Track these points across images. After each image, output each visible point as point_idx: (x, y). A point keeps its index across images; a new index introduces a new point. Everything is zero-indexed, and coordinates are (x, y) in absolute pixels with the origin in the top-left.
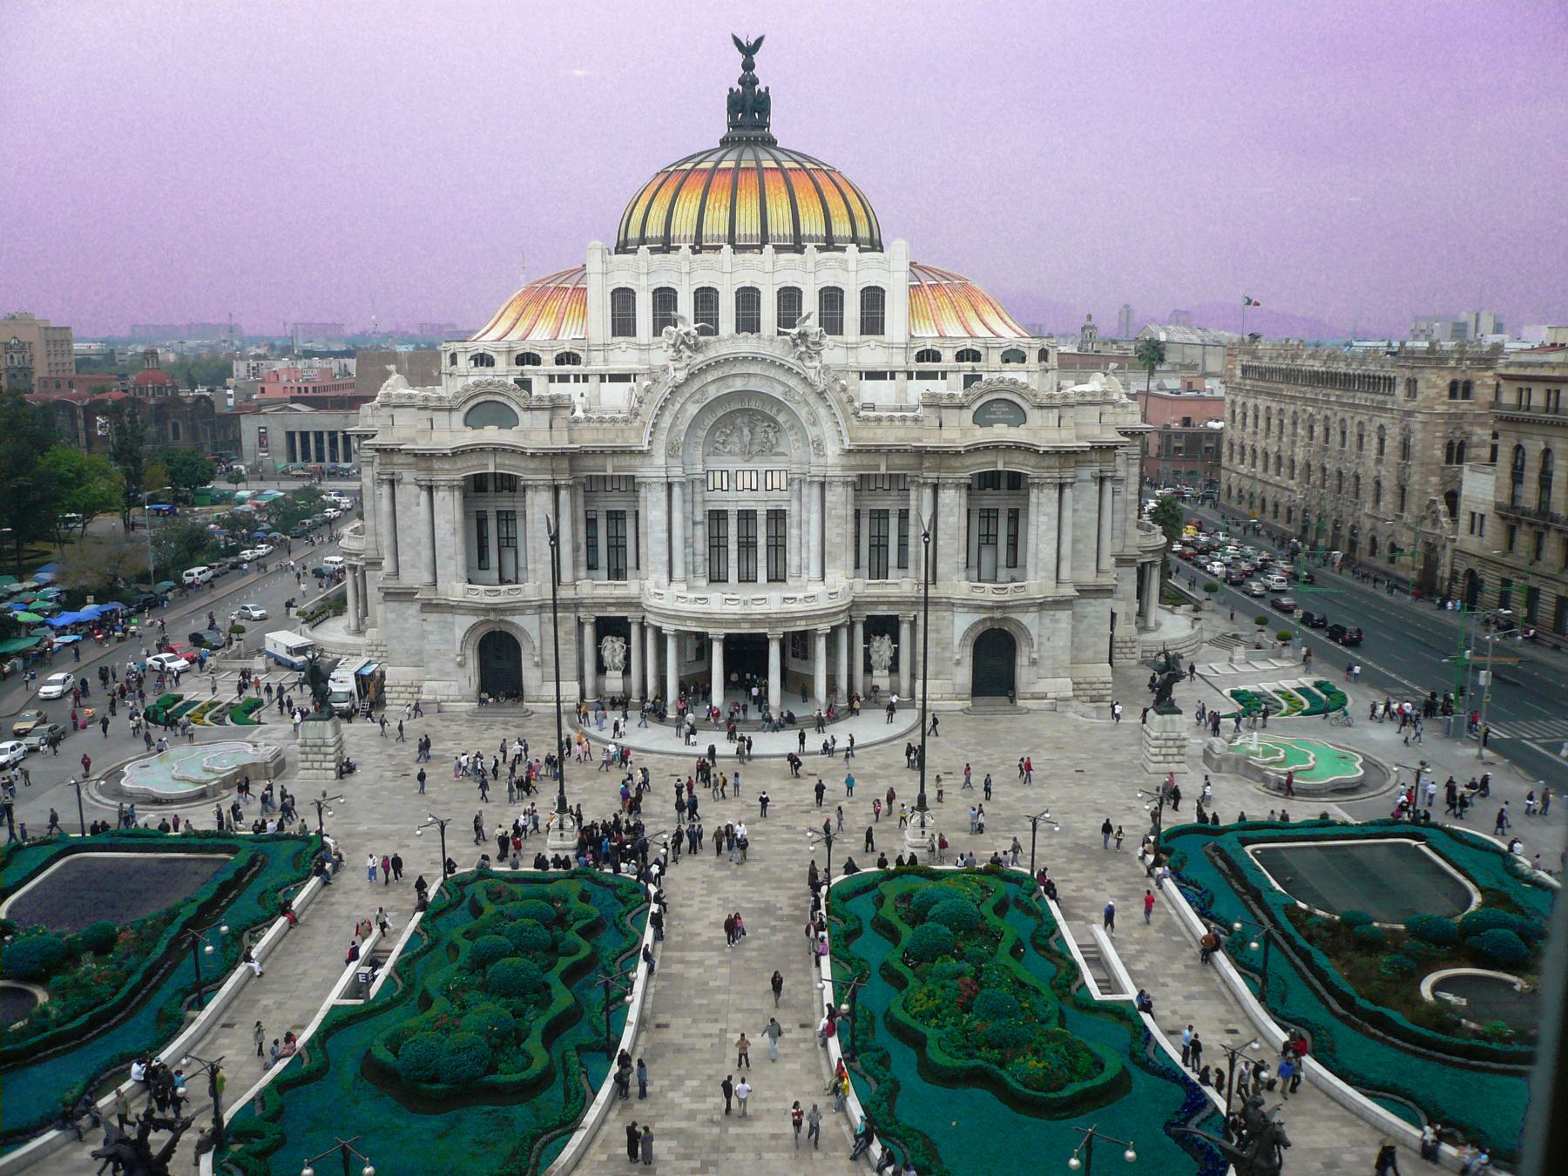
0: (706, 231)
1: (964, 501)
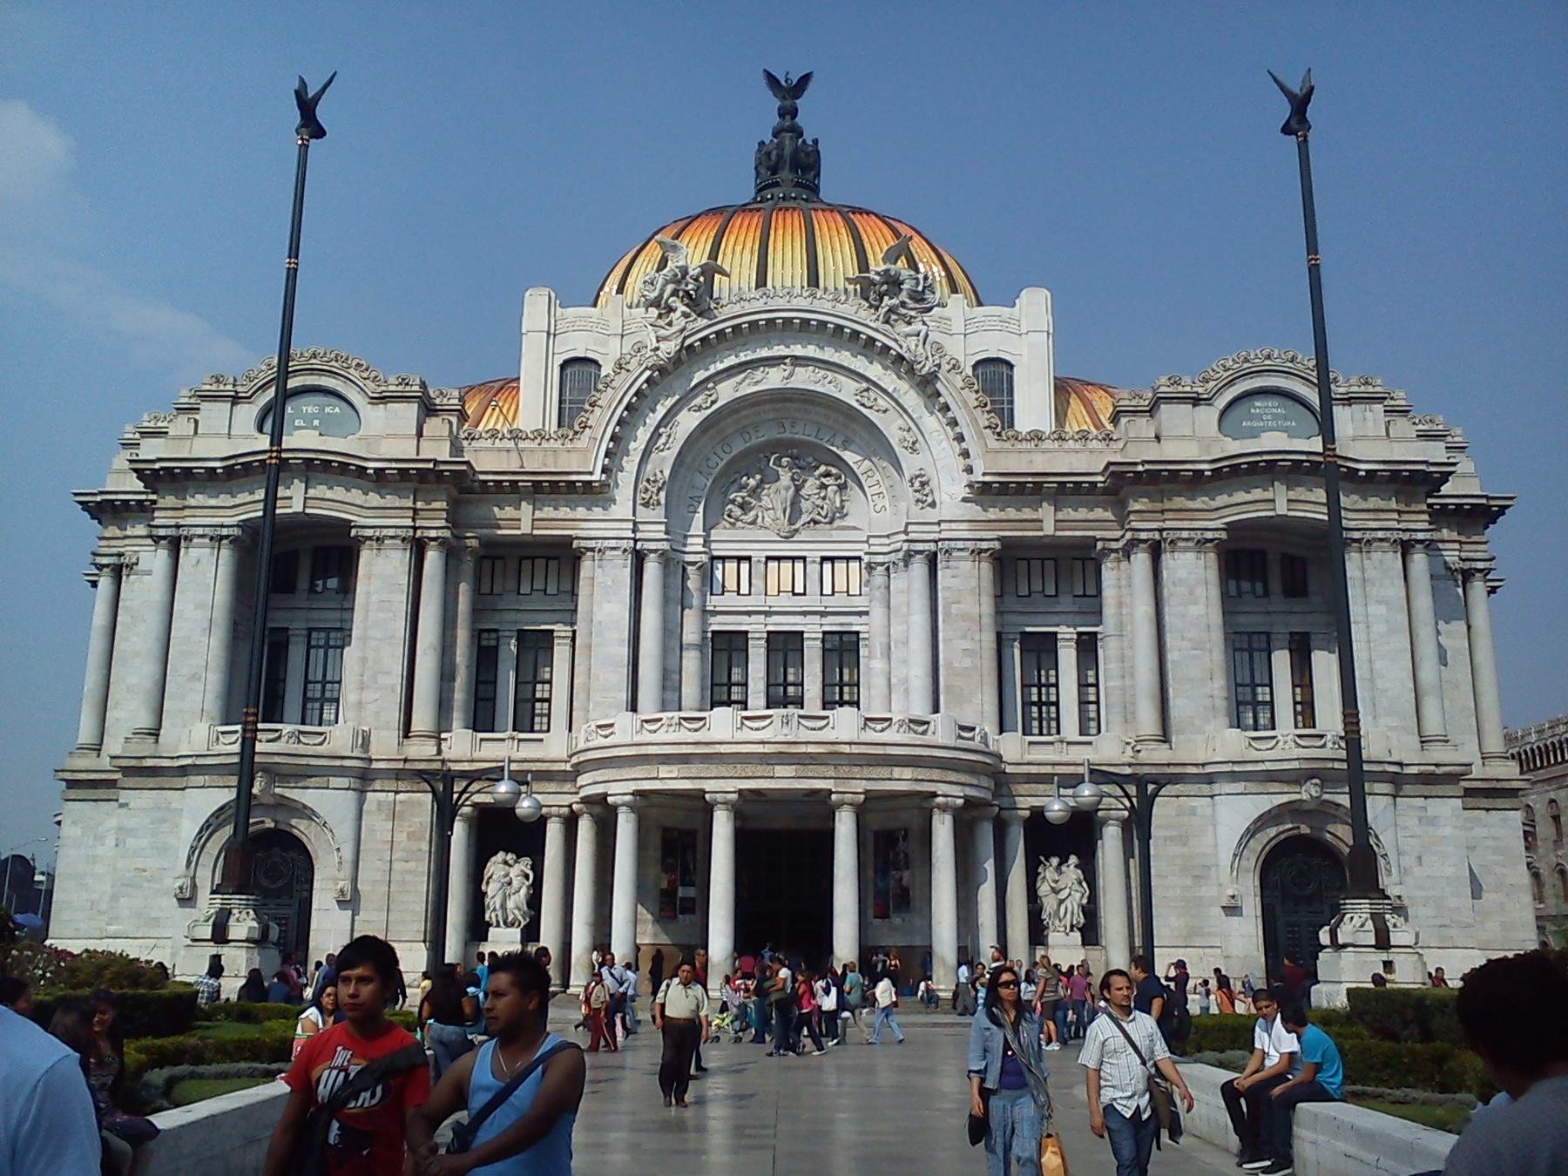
1: (1213, 575)
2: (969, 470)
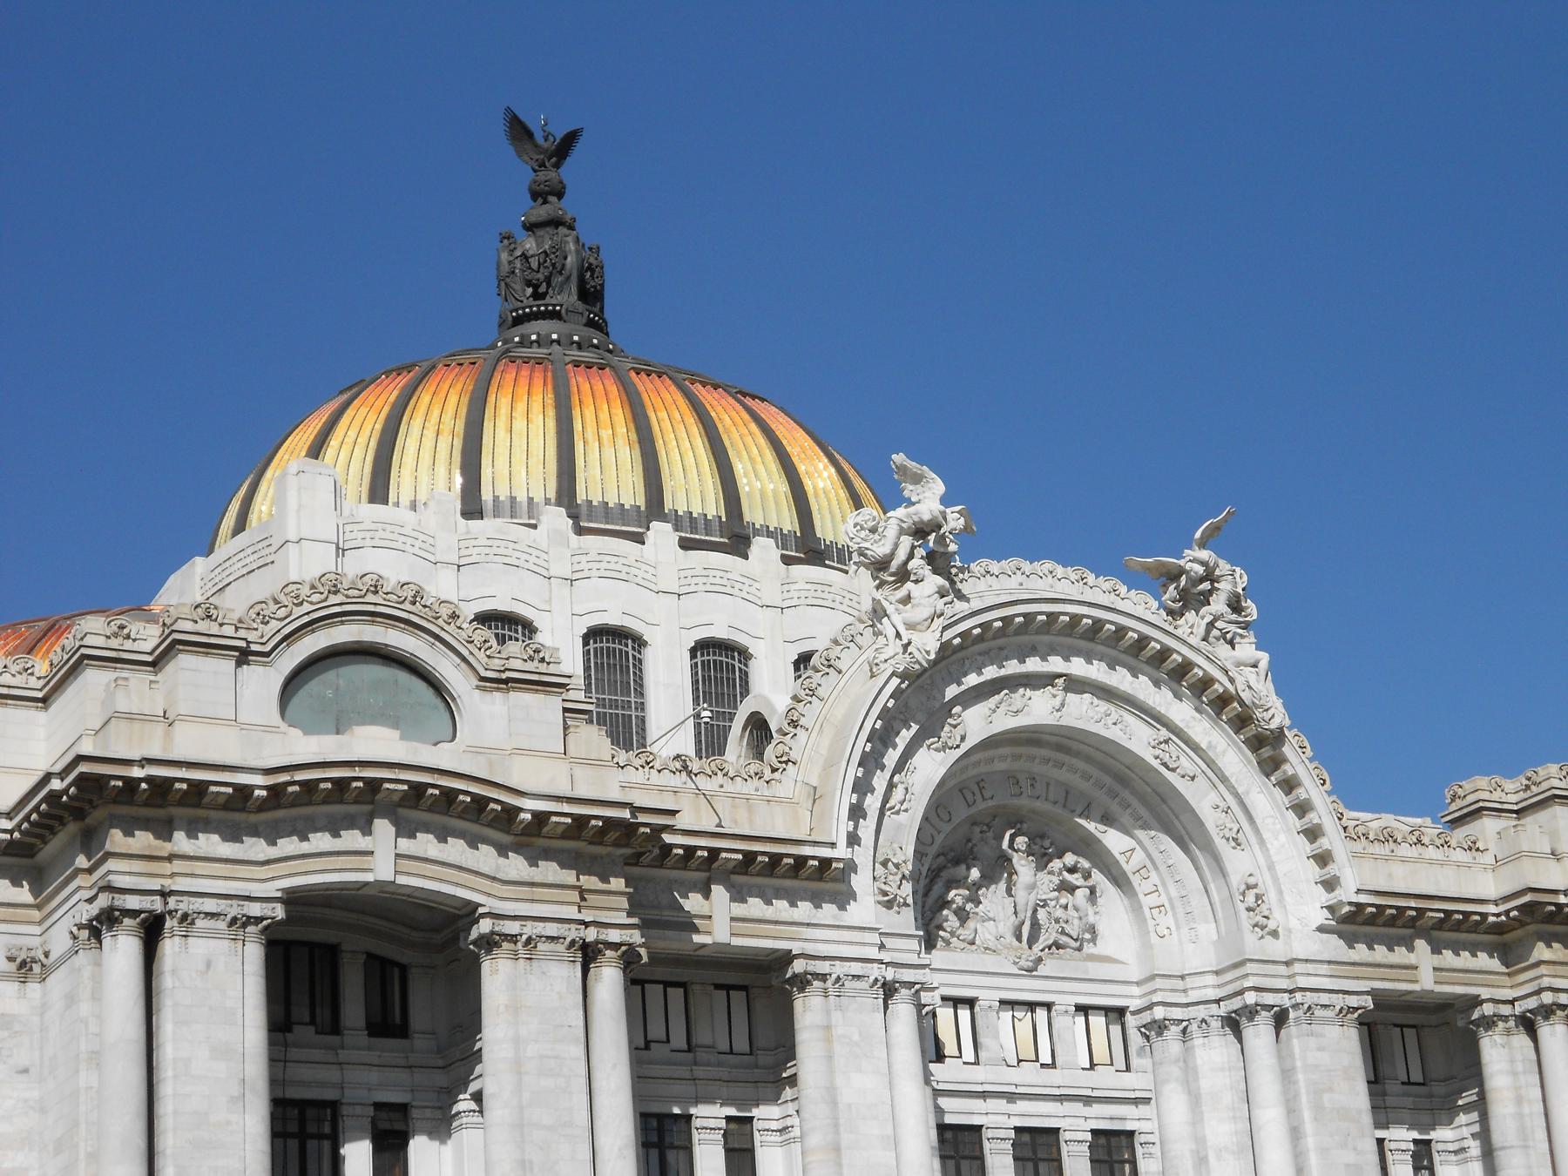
0: (589, 487)
2: (1330, 884)
